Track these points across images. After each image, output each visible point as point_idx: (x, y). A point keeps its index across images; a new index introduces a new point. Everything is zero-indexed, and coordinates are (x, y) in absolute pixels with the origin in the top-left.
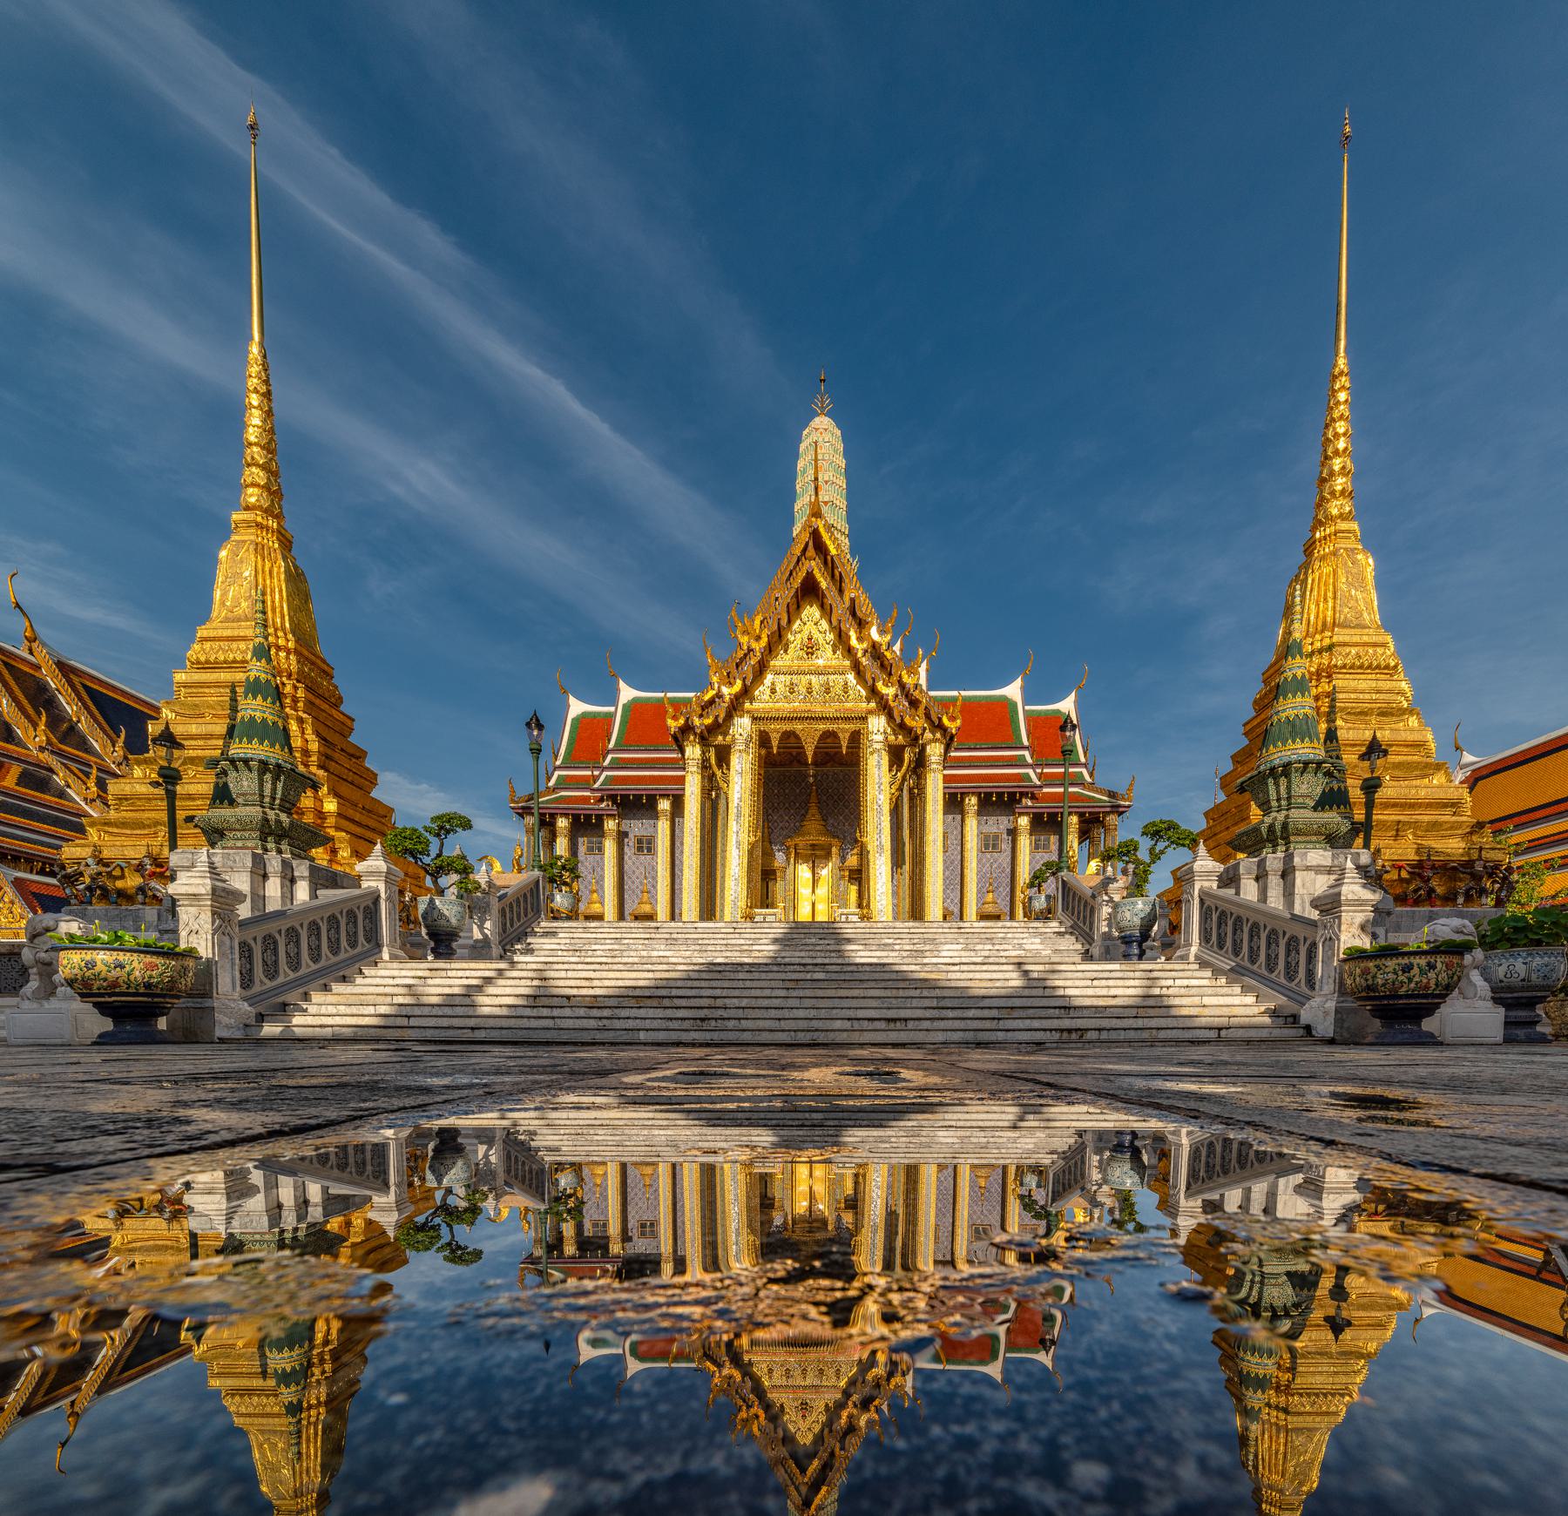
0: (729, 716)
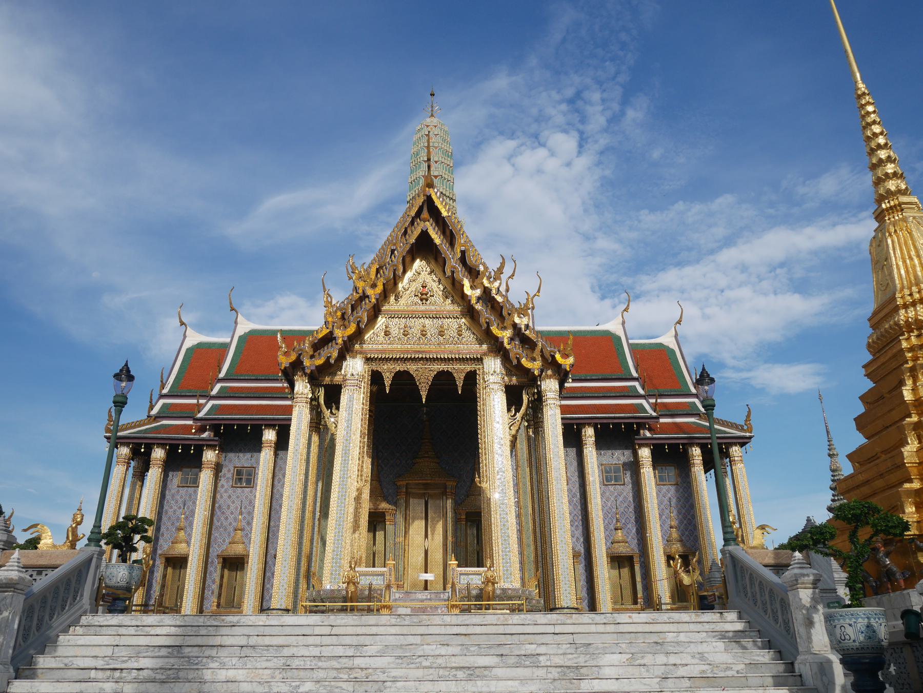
0: (342, 357)
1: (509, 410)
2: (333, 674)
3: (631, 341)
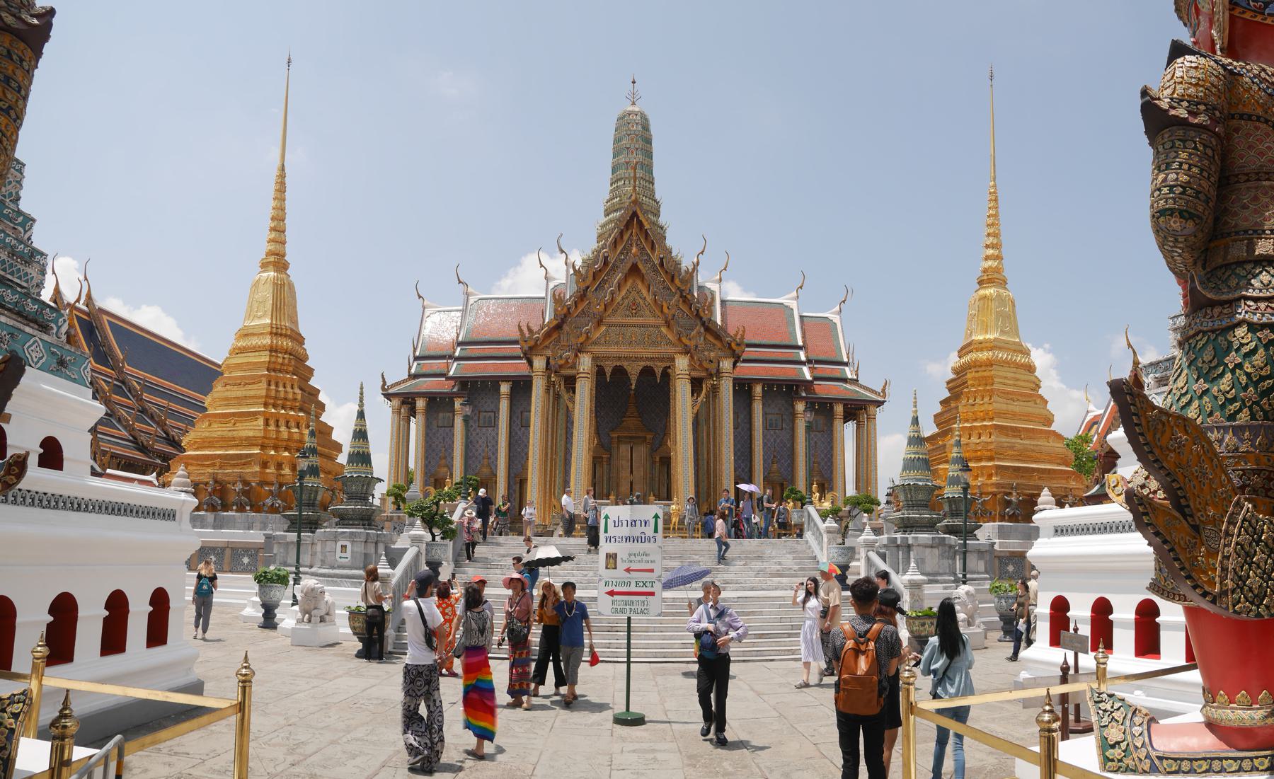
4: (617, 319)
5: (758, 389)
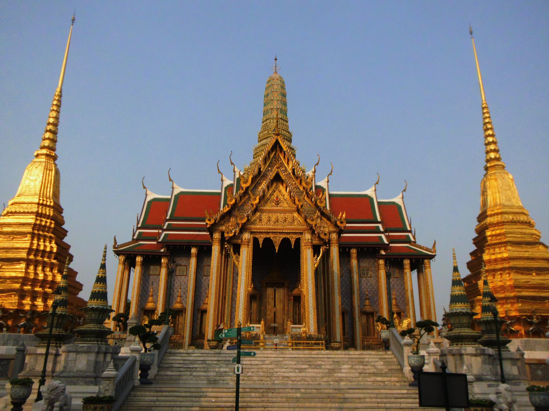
1: (314, 256)
2: (257, 370)
3: (379, 200)
4: (267, 207)
5: (354, 251)
